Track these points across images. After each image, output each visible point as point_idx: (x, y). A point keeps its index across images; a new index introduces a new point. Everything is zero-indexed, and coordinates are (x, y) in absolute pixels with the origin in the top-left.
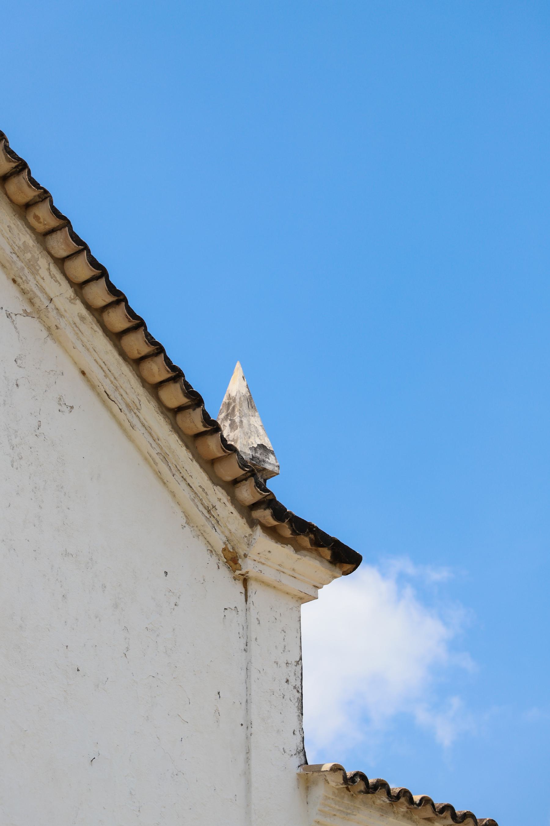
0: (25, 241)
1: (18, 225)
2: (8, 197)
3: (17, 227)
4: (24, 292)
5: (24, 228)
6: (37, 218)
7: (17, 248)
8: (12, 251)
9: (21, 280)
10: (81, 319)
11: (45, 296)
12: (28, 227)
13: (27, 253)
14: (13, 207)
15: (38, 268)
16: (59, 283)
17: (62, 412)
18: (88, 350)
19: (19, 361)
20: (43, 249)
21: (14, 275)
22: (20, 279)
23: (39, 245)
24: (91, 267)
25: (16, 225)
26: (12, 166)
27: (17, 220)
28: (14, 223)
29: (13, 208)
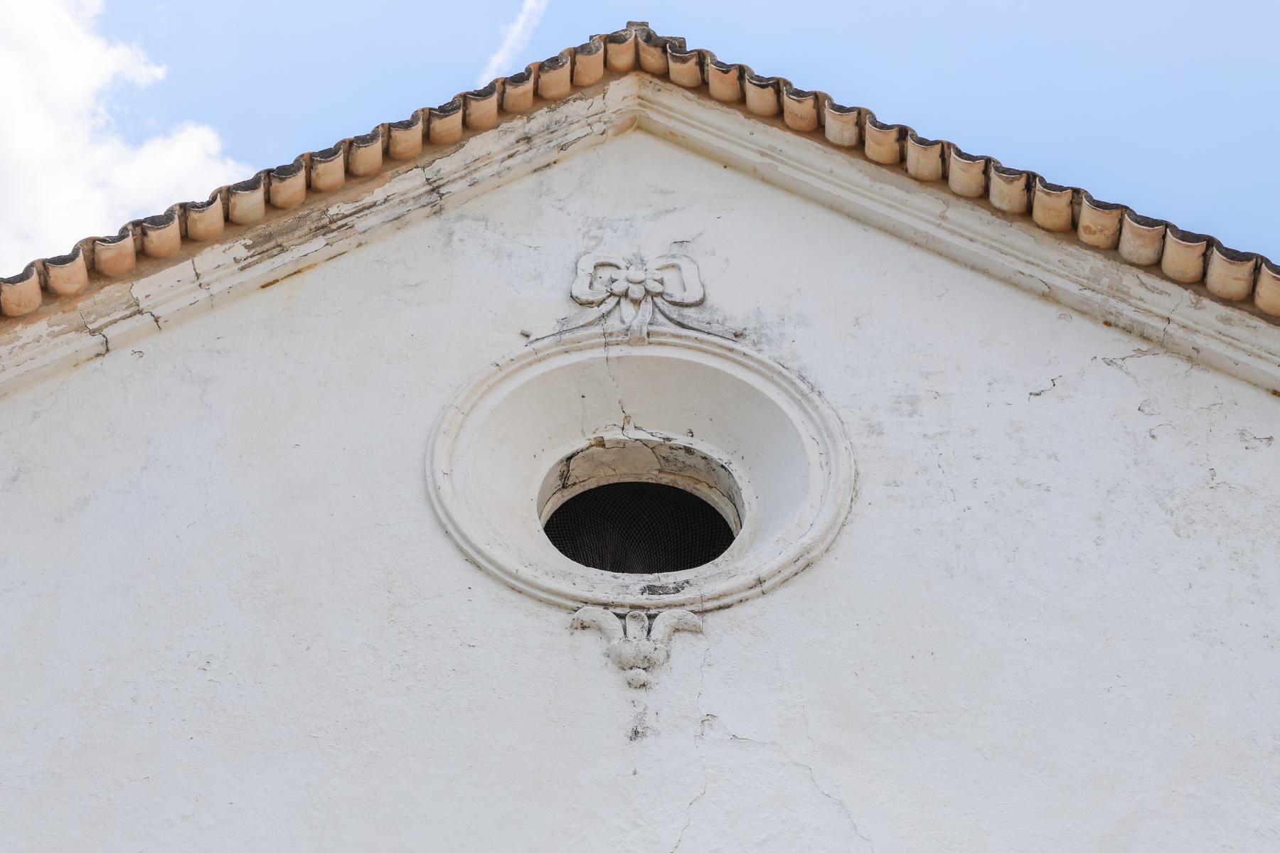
0: (1091, 268)
1: (1071, 252)
2: (1043, 229)
3: (1071, 254)
4: (1128, 330)
6: (1087, 229)
7: (1085, 281)
8: (1081, 288)
9: (1113, 317)
10: (1226, 323)
11: (1157, 319)
12: (1086, 249)
13: (1101, 280)
15: (1125, 290)
16: (1167, 293)
17: (1253, 448)
18: (1260, 357)
19: (1146, 410)
20: (1121, 263)
22: (1110, 316)
23: (1111, 262)
24: (1184, 243)
26: (1021, 189)
27: (1066, 247)
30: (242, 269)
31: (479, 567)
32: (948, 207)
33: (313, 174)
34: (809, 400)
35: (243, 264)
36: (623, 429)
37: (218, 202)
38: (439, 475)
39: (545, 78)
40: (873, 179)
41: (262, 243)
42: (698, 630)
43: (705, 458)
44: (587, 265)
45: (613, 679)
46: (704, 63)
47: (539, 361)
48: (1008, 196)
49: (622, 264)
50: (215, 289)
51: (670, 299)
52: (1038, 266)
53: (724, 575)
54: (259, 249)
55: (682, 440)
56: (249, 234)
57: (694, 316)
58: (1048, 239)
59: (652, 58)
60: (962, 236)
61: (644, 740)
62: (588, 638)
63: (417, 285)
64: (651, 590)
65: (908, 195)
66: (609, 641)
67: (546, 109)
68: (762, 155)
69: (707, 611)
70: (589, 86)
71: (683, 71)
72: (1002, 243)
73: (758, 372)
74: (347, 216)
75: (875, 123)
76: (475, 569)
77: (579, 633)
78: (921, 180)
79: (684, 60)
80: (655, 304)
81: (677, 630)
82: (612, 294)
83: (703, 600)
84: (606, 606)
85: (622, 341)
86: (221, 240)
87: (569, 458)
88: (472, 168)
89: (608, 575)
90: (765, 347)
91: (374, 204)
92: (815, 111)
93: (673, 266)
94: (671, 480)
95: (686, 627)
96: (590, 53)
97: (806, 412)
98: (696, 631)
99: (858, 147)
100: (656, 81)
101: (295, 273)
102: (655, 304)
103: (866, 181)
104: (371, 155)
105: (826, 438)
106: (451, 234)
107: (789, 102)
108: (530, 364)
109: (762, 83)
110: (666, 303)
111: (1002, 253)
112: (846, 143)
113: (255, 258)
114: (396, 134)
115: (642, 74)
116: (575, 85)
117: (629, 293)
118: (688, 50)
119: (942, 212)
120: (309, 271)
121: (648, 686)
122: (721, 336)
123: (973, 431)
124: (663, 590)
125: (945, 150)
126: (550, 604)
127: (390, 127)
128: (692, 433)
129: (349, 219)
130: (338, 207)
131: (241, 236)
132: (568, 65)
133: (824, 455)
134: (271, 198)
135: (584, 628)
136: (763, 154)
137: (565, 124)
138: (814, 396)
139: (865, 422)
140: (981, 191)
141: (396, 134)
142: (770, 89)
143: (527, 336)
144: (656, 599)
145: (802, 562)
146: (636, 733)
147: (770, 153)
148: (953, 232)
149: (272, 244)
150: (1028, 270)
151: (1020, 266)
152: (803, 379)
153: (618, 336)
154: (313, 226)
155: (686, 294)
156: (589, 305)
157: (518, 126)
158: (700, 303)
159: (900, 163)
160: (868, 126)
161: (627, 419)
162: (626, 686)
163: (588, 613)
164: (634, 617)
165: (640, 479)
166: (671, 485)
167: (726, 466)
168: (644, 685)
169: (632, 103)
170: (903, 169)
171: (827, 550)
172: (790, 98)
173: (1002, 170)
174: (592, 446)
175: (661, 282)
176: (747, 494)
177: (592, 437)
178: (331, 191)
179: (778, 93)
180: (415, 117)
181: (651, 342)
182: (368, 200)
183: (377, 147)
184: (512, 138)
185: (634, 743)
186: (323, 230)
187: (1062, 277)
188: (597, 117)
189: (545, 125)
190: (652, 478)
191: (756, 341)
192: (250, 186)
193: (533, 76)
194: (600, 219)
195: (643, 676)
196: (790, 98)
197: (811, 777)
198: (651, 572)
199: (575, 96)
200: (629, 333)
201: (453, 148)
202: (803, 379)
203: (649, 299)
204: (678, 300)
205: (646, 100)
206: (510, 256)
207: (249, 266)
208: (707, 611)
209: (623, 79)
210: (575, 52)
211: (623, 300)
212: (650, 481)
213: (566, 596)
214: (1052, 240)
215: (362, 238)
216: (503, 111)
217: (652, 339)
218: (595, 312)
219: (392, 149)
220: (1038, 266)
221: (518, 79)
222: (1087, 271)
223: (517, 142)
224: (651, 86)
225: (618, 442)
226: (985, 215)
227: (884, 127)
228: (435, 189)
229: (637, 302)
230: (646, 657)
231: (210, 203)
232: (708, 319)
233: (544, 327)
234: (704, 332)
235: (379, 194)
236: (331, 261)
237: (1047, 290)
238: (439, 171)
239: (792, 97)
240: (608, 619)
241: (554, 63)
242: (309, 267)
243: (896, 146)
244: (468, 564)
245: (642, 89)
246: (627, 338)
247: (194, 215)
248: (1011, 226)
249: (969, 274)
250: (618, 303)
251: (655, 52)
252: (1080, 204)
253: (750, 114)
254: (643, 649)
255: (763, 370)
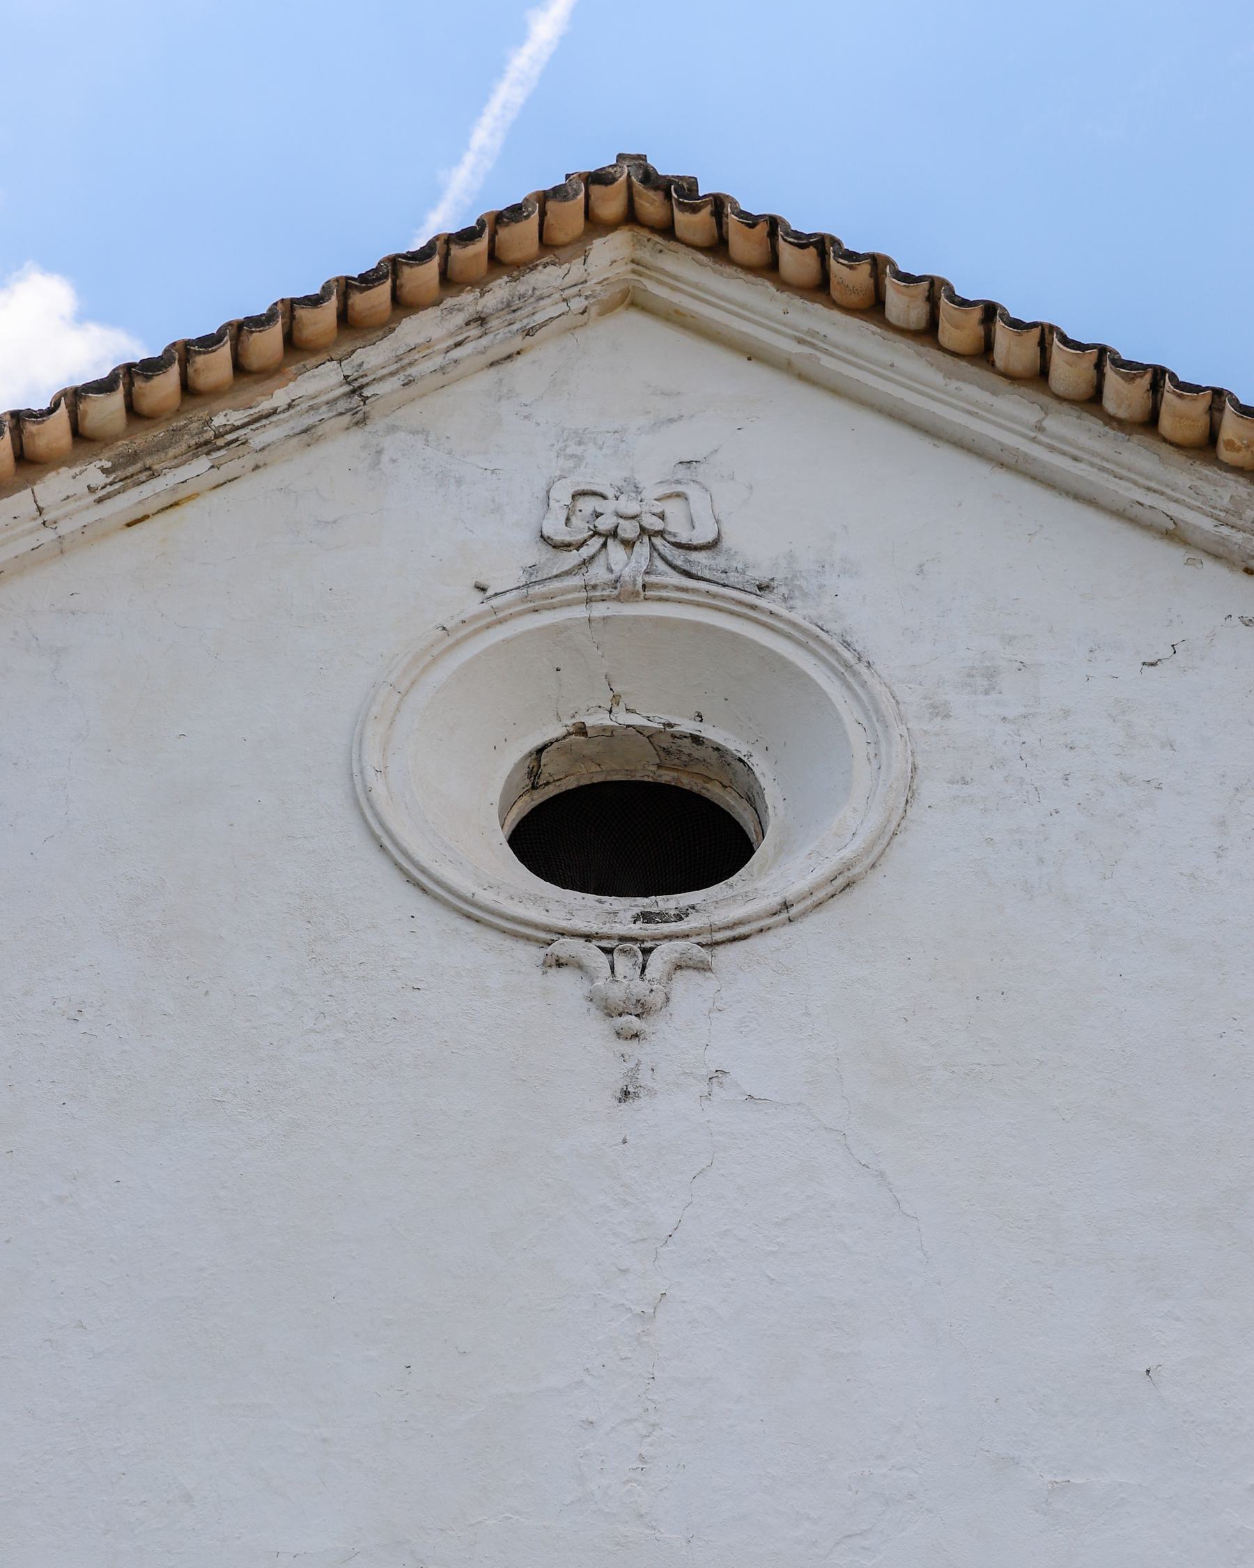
1: (1206, 476)
2: (1171, 444)
3: (1206, 479)
5: (1219, 474)
6: (1230, 445)
8: (1216, 523)
13: (1244, 512)
14: (1186, 453)
21: (1243, 561)
25: (1204, 478)
26: (1145, 390)
27: (1200, 469)
28: (1198, 478)
29: (1187, 456)
30: (100, 501)
31: (424, 890)
32: (1046, 414)
33: (190, 370)
34: (855, 674)
35: (101, 493)
36: (610, 712)
37: (63, 410)
38: (370, 773)
39: (503, 233)
40: (949, 375)
41: (125, 466)
42: (705, 967)
43: (717, 749)
44: (562, 495)
45: (600, 1027)
46: (723, 213)
47: (500, 622)
48: (1127, 399)
49: (610, 493)
50: (64, 528)
51: (673, 540)
52: (1162, 494)
53: (740, 898)
54: (121, 474)
55: (687, 726)
56: (107, 453)
57: (705, 562)
58: (1177, 457)
59: (651, 205)
60: (1064, 453)
61: (637, 1102)
62: (564, 980)
63: (335, 522)
64: (647, 917)
65: (995, 398)
66: (592, 982)
67: (505, 278)
68: (799, 342)
69: (717, 943)
70: (565, 245)
71: (692, 224)
72: (1117, 464)
73: (788, 637)
74: (238, 428)
75: (953, 297)
76: (420, 893)
77: (553, 971)
78: (1011, 377)
79: (695, 209)
80: (653, 546)
81: (679, 967)
82: (596, 533)
83: (712, 929)
84: (588, 937)
85: (609, 596)
86: (68, 462)
87: (540, 751)
88: (406, 361)
89: (591, 898)
90: (798, 603)
91: (274, 412)
92: (872, 281)
93: (678, 495)
94: (674, 778)
95: (691, 963)
96: (565, 198)
97: (849, 687)
98: (703, 968)
99: (928, 332)
100: (657, 238)
101: (171, 506)
102: (653, 546)
103: (938, 379)
104: (269, 341)
105: (876, 723)
106: (379, 452)
107: (837, 268)
108: (488, 627)
109: (801, 241)
110: (667, 545)
111: (1115, 477)
112: (913, 326)
113: (116, 486)
114: (303, 313)
115: (637, 229)
116: (546, 245)
117: (619, 531)
118: (701, 194)
119: (1038, 421)
120: (192, 503)
121: (641, 1037)
122: (739, 589)
123: (1067, 713)
124: (663, 918)
125: (1046, 335)
126: (516, 935)
127: (292, 305)
128: (701, 717)
129: (242, 432)
130: (225, 416)
131: (96, 455)
132: (535, 216)
133: (872, 745)
134: (135, 404)
135: (559, 965)
136: (801, 341)
137: (532, 300)
138: (861, 668)
139: (927, 702)
140: (1091, 392)
141: (303, 313)
142: (812, 250)
143: (484, 590)
144: (652, 929)
145: (840, 881)
146: (626, 1093)
147: (809, 339)
148: (1052, 449)
149: (139, 466)
150: (1148, 499)
151: (1139, 495)
152: (847, 645)
153: (603, 589)
154: (192, 442)
155: (694, 532)
156: (565, 548)
157: (468, 301)
158: (712, 546)
159: (984, 353)
160: (944, 301)
161: (616, 699)
162: (615, 1037)
163: (566, 948)
164: (623, 951)
165: (632, 777)
166: (673, 784)
167: (745, 759)
168: (636, 1035)
169: (623, 270)
170: (988, 361)
171: (873, 866)
172: (838, 262)
173: (1119, 363)
174: (569, 734)
175: (662, 516)
176: (772, 795)
177: (570, 722)
178: (215, 393)
179: (823, 256)
180: (326, 289)
181: (647, 597)
182: (266, 405)
183: (275, 332)
184: (460, 318)
185: (623, 1105)
186: (206, 447)
187: (1192, 509)
188: (576, 289)
189: (505, 300)
190: (648, 776)
191: (786, 596)
192: (104, 386)
193: (487, 231)
194: (581, 431)
195: (634, 1023)
196: (838, 262)
197: (845, 1144)
198: (646, 896)
199: (545, 260)
200: (618, 585)
201: (380, 333)
202: (847, 645)
203: (646, 539)
204: (684, 541)
205: (643, 266)
206: (459, 482)
207: (108, 496)
208: (717, 943)
209: (610, 236)
210: (544, 198)
211: (610, 541)
212: (646, 779)
213: (537, 926)
214: (1183, 459)
215: (259, 458)
216: (449, 281)
217: (649, 593)
218: (573, 558)
219: (296, 334)
220: (1162, 494)
221: (467, 236)
222: (1226, 500)
223: (467, 324)
224: (650, 245)
225: (604, 729)
226: (1096, 425)
227: (964, 303)
228: (355, 389)
229: (629, 544)
230: (638, 1001)
231: (51, 411)
232: (723, 566)
233: (505, 577)
234: (718, 583)
235: (280, 398)
236: (219, 490)
237: (1171, 526)
238: (361, 365)
239: (841, 261)
240: (591, 954)
241: (515, 213)
242: (189, 498)
243: (980, 330)
244: (410, 886)
245: (637, 250)
246: (616, 592)
247: (30, 427)
248: (1129, 440)
249: (1070, 506)
250: (604, 545)
251: (655, 197)
252: (1222, 410)
253: (784, 285)
254: (635, 991)
255: (793, 632)
